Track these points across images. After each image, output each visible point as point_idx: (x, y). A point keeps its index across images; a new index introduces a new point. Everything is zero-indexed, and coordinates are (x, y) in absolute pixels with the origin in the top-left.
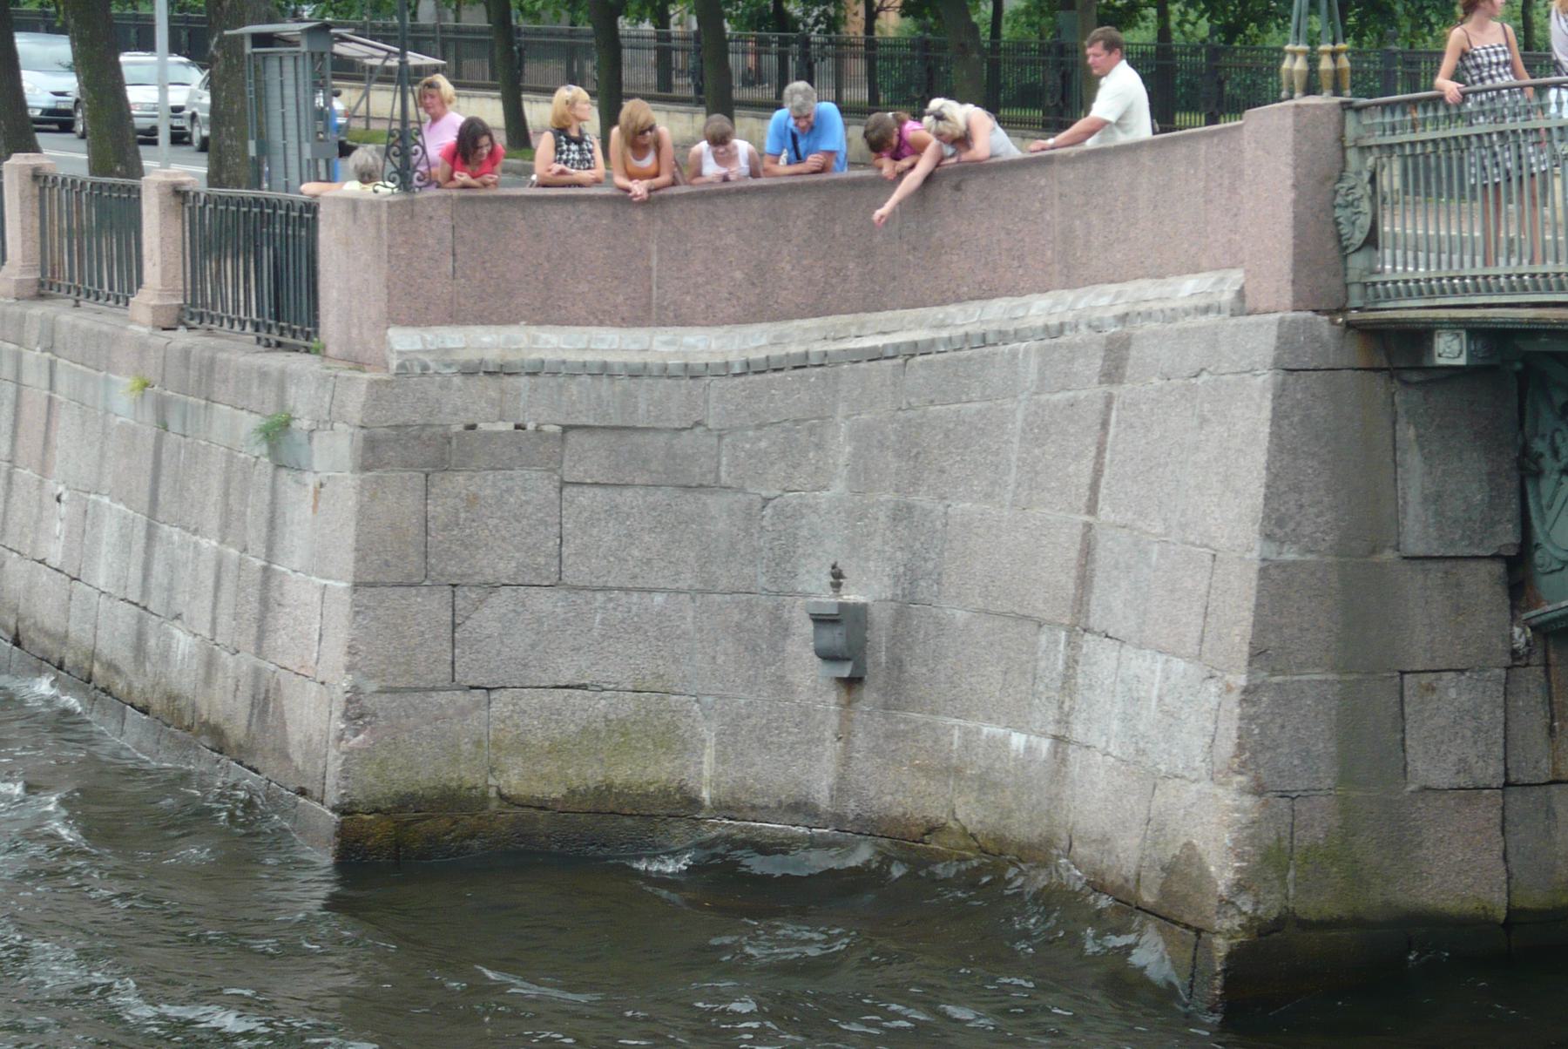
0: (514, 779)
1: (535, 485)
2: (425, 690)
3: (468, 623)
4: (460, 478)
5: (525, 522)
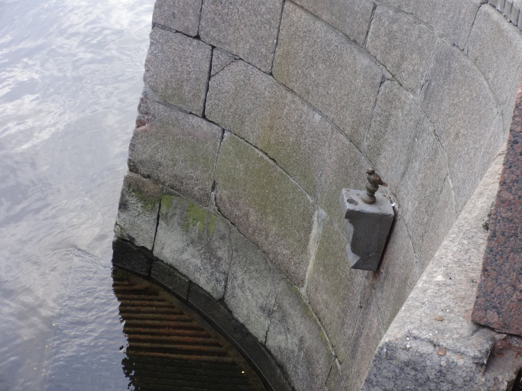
2: (185, 112)
3: (217, 77)
5: (259, 18)
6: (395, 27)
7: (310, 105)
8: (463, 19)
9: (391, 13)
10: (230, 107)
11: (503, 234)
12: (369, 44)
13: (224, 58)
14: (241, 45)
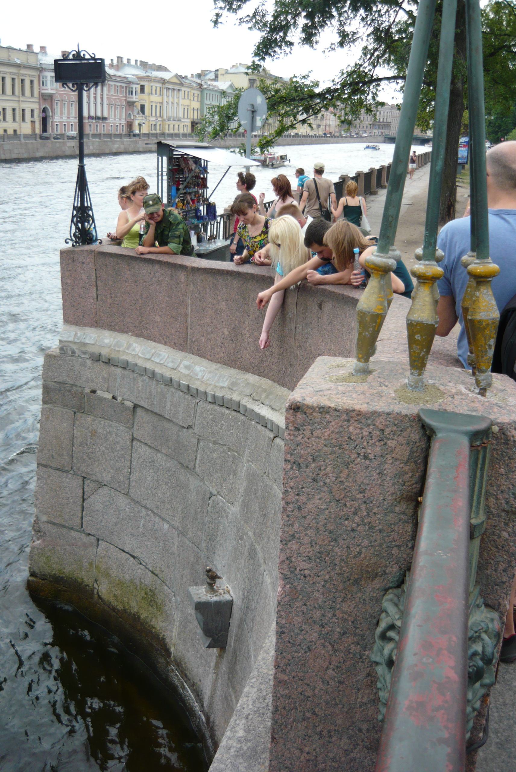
0: (104, 589)
1: (119, 433)
3: (89, 499)
4: (89, 419)
5: (116, 453)
6: (215, 455)
7: (160, 516)
8: (263, 449)
9: (211, 445)
10: (101, 521)
11: (284, 708)
12: (197, 469)
13: (93, 485)
14: (104, 475)
